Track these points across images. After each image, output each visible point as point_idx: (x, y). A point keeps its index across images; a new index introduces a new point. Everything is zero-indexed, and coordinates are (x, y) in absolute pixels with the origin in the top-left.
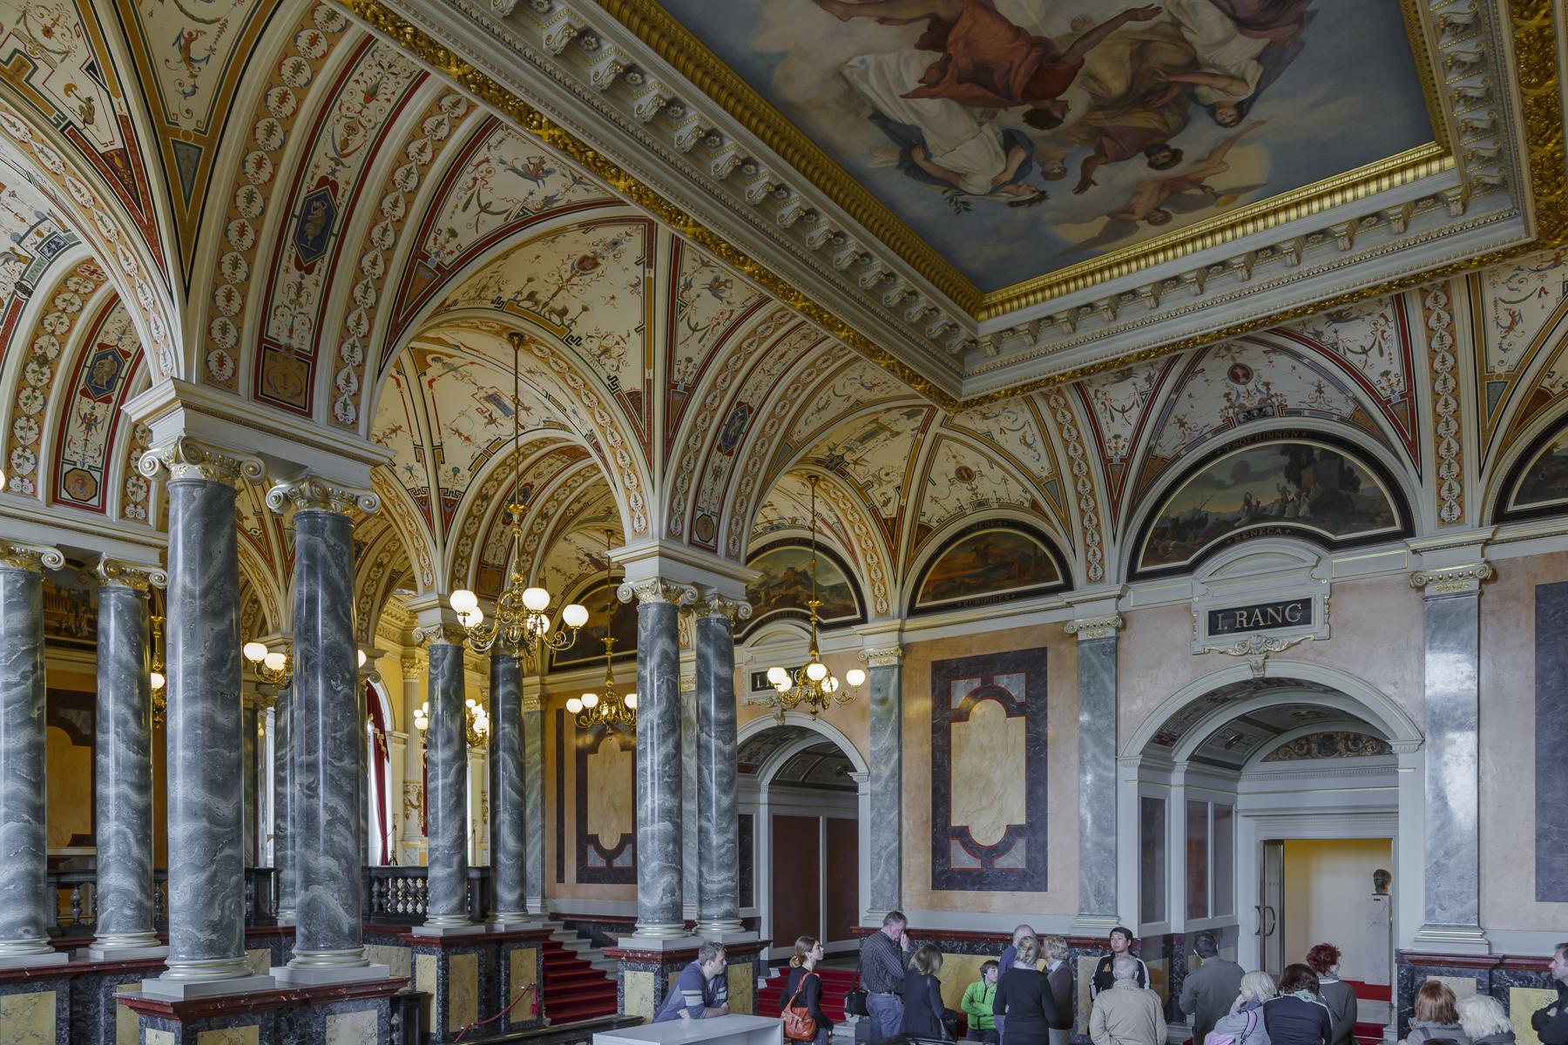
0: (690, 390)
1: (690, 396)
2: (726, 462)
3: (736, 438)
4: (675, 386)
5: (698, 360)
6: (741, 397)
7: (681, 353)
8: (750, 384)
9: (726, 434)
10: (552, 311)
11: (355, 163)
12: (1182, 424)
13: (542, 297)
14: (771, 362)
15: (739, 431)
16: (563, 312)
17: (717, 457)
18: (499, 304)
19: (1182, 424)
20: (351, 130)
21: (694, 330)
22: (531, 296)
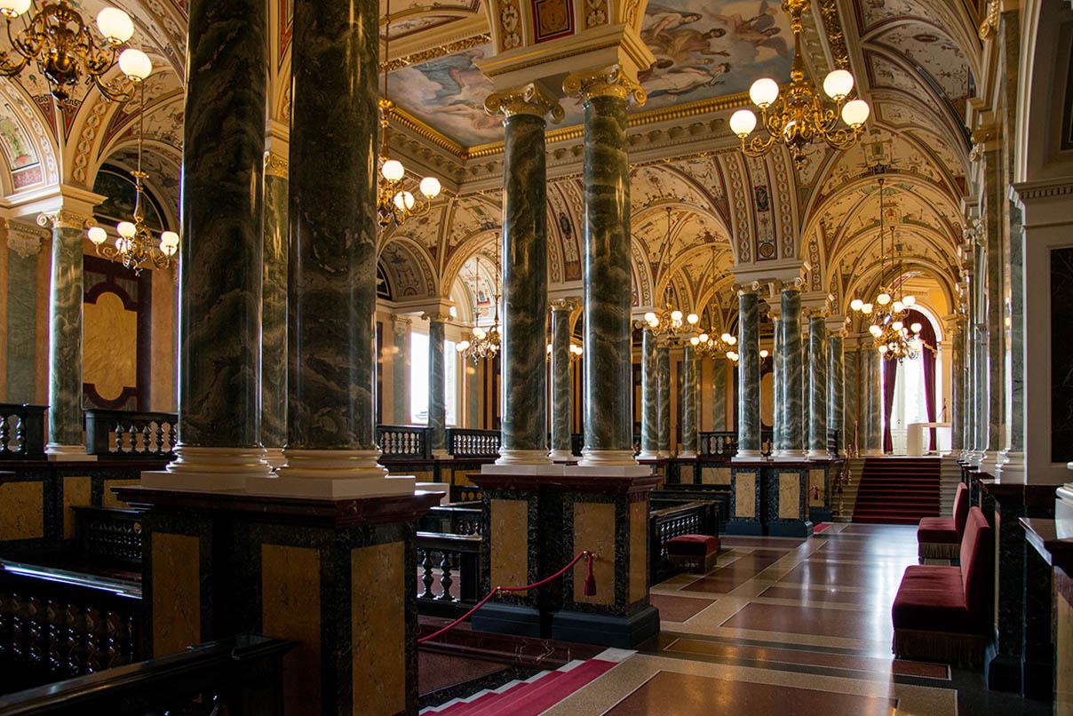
0: (725, 196)
1: (727, 200)
2: (768, 215)
3: (766, 203)
4: (716, 199)
5: (718, 184)
6: (755, 183)
7: (708, 187)
8: (753, 178)
9: (759, 204)
10: (667, 196)
11: (563, 204)
12: (949, 75)
13: (658, 194)
14: (753, 164)
15: (766, 197)
16: (670, 195)
17: (760, 216)
18: (648, 205)
19: (949, 75)
20: (556, 199)
21: (705, 177)
22: (654, 197)
